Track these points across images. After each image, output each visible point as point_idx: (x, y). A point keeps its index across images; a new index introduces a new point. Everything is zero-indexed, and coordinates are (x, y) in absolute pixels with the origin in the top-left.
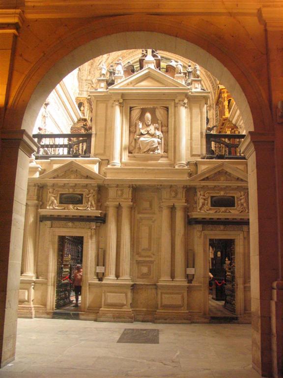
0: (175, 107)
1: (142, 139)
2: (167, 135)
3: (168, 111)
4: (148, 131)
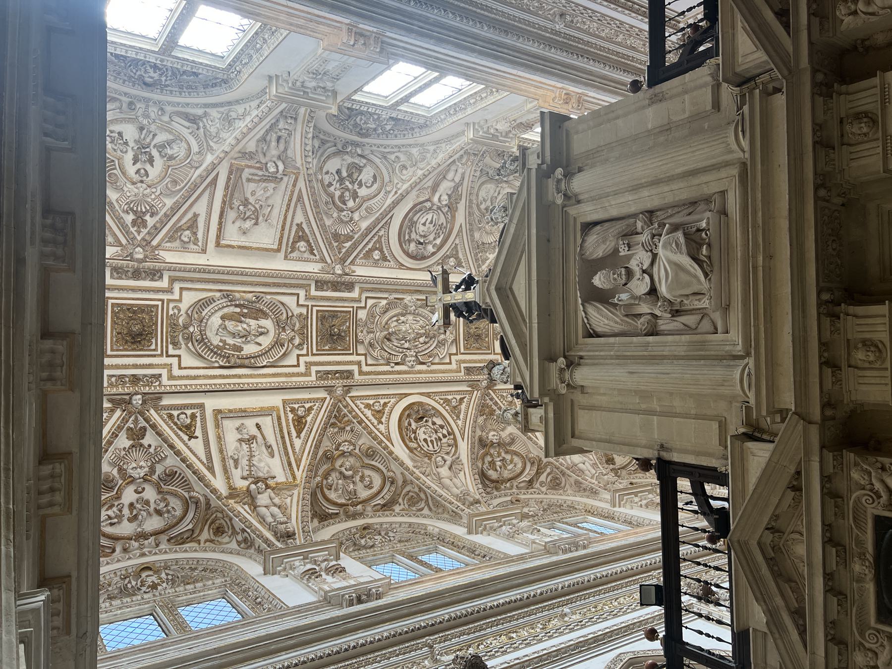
0: (579, 202)
1: (663, 289)
2: (658, 213)
3: (596, 224)
4: (644, 272)
